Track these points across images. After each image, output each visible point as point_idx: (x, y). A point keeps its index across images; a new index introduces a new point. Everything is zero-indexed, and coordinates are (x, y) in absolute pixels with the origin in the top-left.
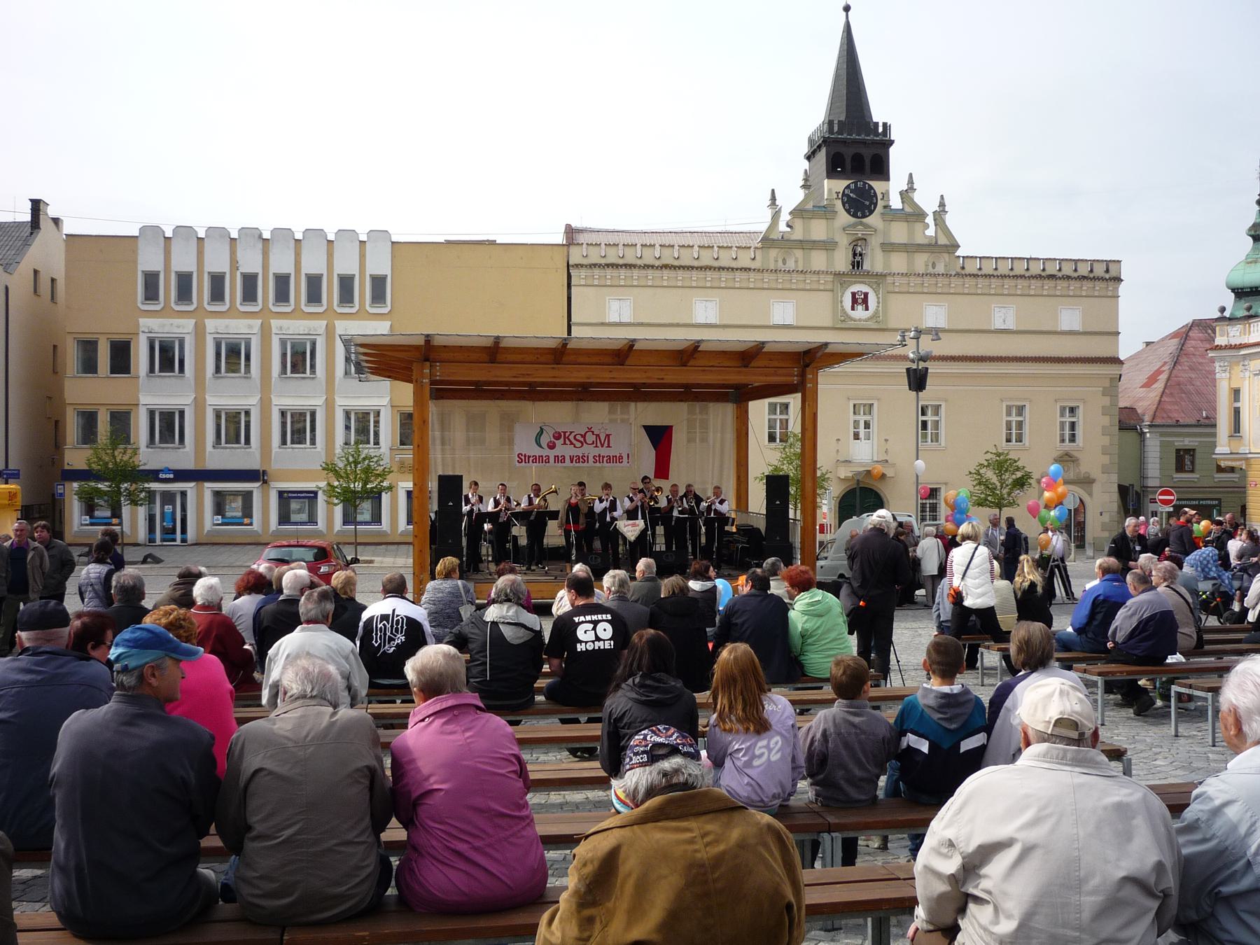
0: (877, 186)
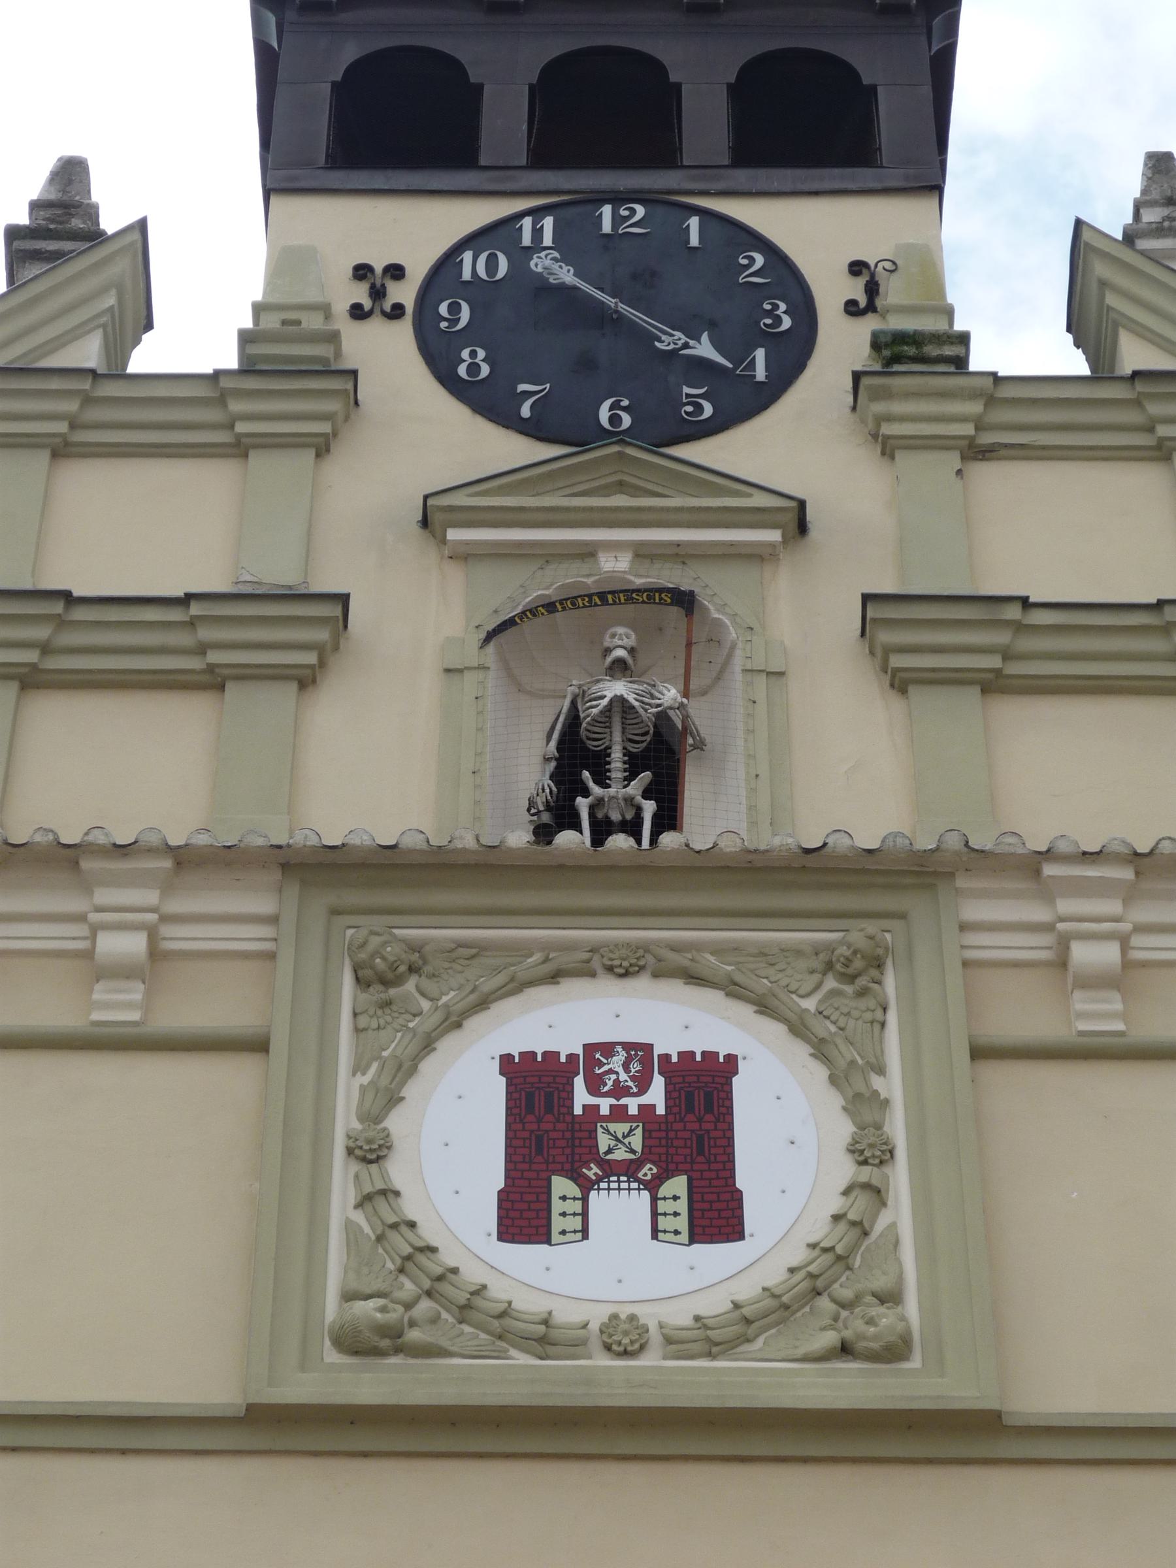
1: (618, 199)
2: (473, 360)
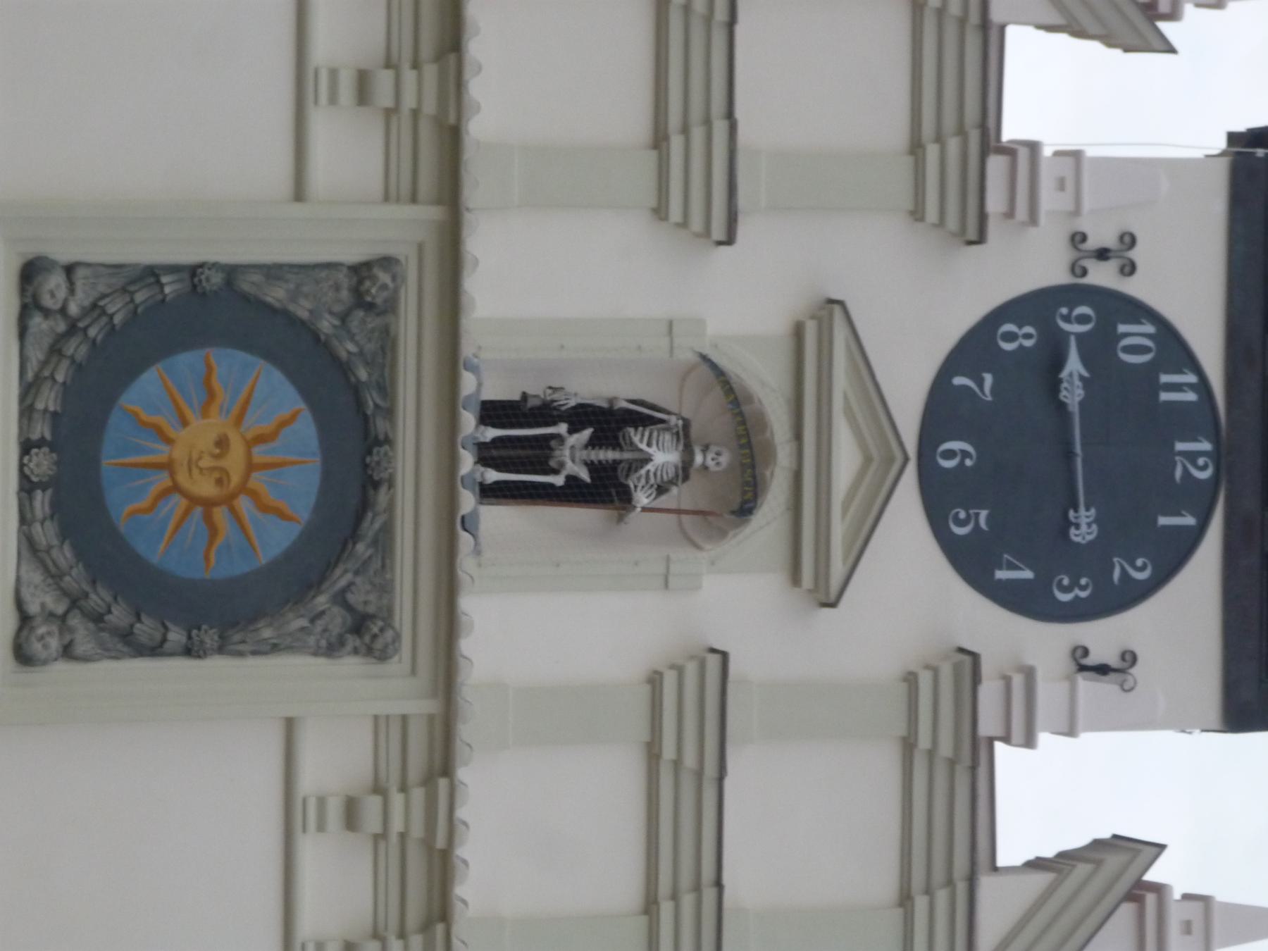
0: (1184, 616)
1: (1216, 456)
2: (1025, 337)
